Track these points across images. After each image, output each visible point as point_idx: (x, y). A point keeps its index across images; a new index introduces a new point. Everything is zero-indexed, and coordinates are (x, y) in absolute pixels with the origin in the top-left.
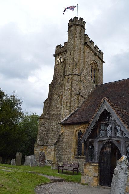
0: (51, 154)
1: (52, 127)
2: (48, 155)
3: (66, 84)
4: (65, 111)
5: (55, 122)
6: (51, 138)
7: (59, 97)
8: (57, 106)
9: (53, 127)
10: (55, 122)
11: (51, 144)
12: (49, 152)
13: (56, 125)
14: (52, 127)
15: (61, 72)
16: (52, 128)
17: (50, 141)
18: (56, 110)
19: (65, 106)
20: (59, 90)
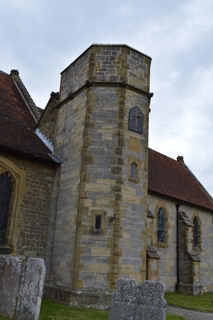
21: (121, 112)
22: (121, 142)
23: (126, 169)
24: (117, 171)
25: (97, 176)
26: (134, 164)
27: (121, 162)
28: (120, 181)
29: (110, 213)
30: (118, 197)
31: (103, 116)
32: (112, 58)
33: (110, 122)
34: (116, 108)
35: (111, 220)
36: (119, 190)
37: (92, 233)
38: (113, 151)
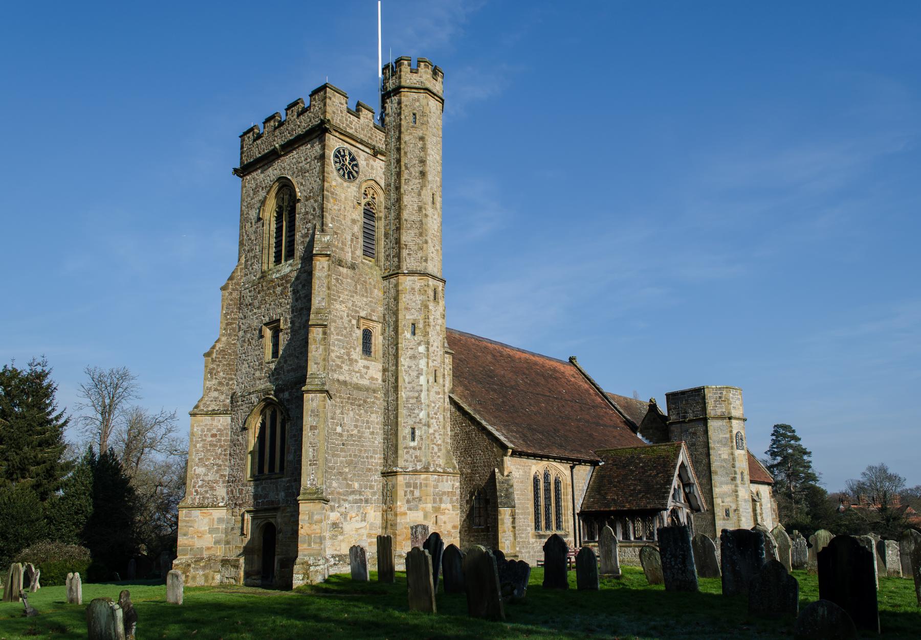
0: (342, 533)
1: (339, 429)
2: (334, 537)
3: (431, 306)
4: (432, 393)
5: (351, 414)
6: (341, 473)
7: (354, 322)
8: (348, 354)
9: (343, 431)
10: (351, 414)
11: (339, 493)
12: (335, 525)
13: (356, 426)
14: (339, 429)
15: (354, 221)
16: (341, 435)
17: (335, 484)
18: (345, 367)
19: (432, 379)
20: (356, 293)
21: (731, 437)
22: (734, 459)
23: (738, 476)
24: (734, 479)
25: (721, 483)
26: (742, 473)
27: (735, 473)
28: (736, 486)
29: (734, 507)
30: (737, 496)
31: (719, 442)
32: (720, 397)
33: (725, 445)
34: (728, 436)
35: (735, 510)
36: (737, 491)
37: (724, 519)
38: (730, 466)
